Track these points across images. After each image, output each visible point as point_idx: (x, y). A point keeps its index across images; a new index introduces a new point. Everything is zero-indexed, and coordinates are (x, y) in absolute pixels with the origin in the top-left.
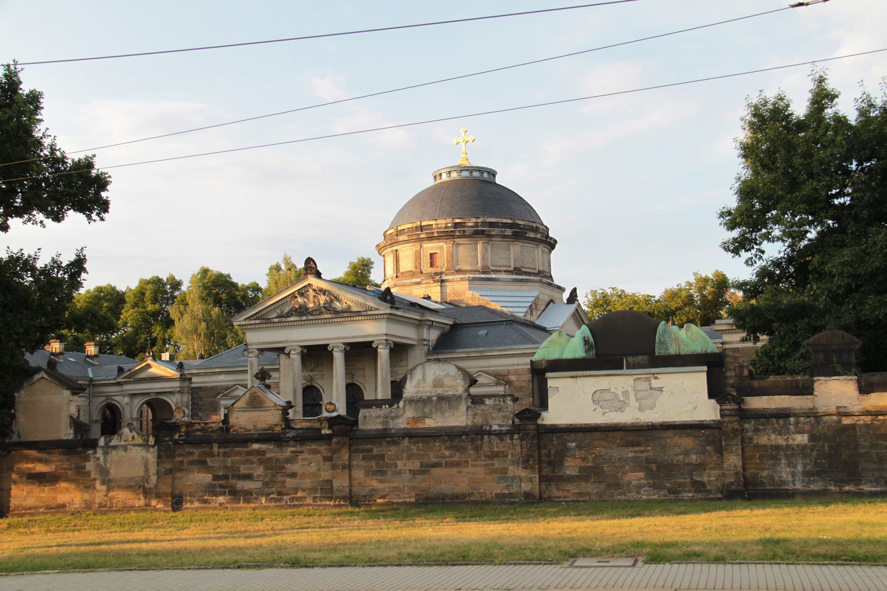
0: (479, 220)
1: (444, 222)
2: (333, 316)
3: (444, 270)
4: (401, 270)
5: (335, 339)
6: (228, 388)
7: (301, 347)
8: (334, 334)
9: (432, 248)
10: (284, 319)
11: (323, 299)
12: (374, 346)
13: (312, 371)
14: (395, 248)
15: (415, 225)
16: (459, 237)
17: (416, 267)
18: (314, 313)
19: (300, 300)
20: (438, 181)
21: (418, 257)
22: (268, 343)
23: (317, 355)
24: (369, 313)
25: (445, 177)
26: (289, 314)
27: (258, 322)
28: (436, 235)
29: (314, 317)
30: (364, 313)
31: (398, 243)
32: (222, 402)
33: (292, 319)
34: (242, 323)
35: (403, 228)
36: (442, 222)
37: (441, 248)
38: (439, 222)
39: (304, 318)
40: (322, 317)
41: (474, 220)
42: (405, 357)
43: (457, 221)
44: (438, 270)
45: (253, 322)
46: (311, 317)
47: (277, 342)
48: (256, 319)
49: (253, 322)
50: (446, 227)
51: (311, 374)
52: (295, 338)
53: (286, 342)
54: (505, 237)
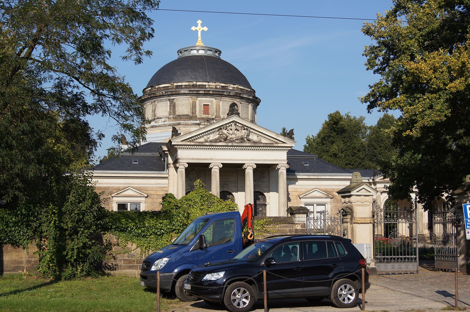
0: (235, 86)
1: (214, 84)
3: (214, 117)
4: (177, 113)
6: (119, 189)
8: (249, 158)
9: (206, 101)
10: (214, 144)
11: (243, 133)
14: (173, 98)
15: (191, 84)
16: (226, 96)
17: (193, 113)
18: (237, 141)
19: (225, 131)
21: (194, 106)
23: (233, 172)
24: (279, 145)
26: (216, 141)
28: (211, 92)
30: (276, 145)
32: (114, 199)
34: (179, 143)
35: (180, 84)
36: (213, 84)
37: (212, 102)
38: (210, 84)
39: (230, 144)
41: (232, 86)
44: (210, 116)
45: (189, 143)
47: (204, 159)
50: (216, 88)
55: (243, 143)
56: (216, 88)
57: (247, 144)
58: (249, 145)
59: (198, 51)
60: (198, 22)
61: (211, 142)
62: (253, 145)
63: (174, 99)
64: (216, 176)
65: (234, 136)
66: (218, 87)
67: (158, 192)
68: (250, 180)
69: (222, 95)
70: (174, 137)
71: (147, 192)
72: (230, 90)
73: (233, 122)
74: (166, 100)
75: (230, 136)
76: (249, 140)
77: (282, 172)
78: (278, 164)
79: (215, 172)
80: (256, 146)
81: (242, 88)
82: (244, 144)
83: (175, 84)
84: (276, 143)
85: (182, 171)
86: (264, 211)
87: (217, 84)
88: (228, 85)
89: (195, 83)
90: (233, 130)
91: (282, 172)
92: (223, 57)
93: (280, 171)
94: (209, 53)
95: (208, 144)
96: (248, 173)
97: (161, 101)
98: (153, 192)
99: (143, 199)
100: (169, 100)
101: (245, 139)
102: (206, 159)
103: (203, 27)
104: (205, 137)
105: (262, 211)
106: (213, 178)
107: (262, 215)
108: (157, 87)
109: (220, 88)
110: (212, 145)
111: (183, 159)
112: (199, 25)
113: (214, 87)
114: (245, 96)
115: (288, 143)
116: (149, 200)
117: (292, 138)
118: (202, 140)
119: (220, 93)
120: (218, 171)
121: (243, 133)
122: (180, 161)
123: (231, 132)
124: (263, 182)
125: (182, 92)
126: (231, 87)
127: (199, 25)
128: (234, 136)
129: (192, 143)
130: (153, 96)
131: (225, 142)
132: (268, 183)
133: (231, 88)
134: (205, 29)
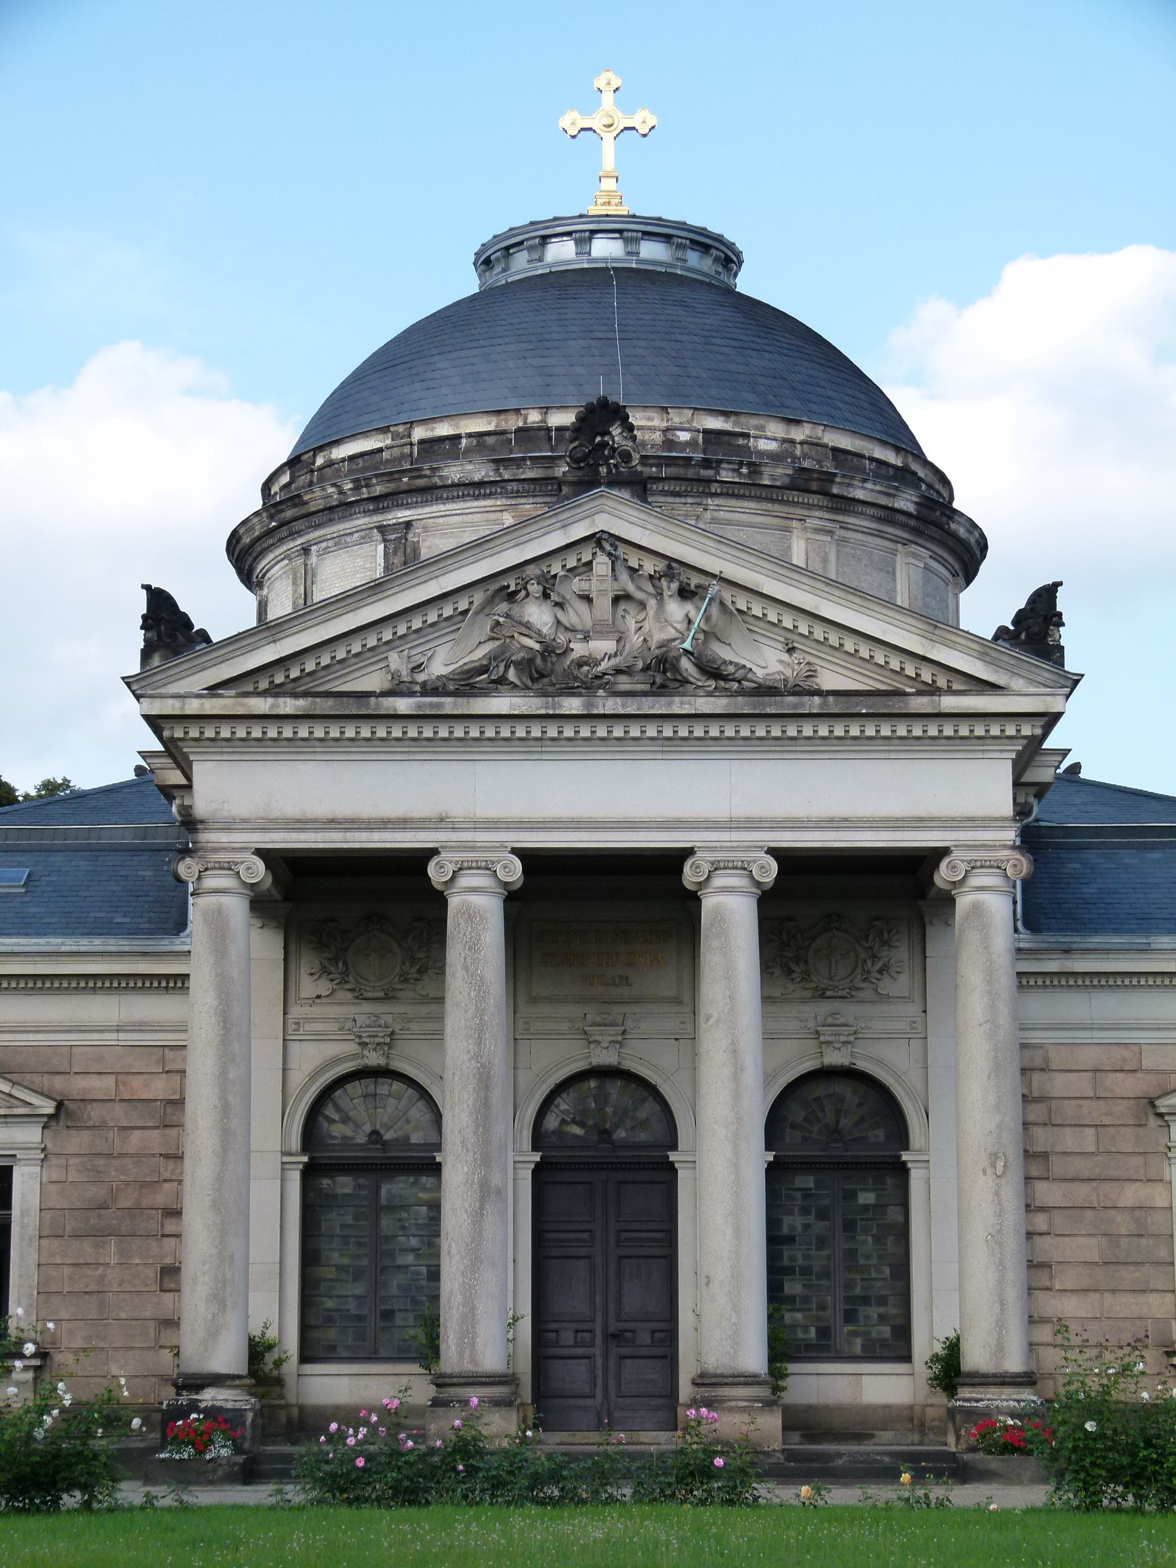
0: (799, 434)
2: (742, 705)
5: (732, 825)
7: (524, 855)
10: (449, 705)
12: (944, 874)
13: (388, 997)
14: (403, 515)
15: (513, 423)
16: (730, 491)
18: (624, 683)
19: (538, 615)
20: (498, 277)
22: (332, 823)
23: (602, 910)
24: (949, 703)
25: (521, 265)
26: (467, 683)
27: (288, 705)
29: (612, 705)
30: (920, 704)
31: (430, 492)
33: (500, 704)
34: (193, 707)
35: (443, 429)
39: (572, 705)
40: (678, 705)
41: (776, 429)
42: (901, 953)
43: (715, 423)
45: (261, 705)
46: (612, 705)
47: (385, 824)
48: (275, 691)
49: (261, 705)
51: (387, 1012)
52: (485, 810)
53: (441, 822)
54: (889, 515)
55: (680, 689)
56: (669, 444)
57: (704, 705)
58: (718, 705)
59: (583, 240)
60: (600, 82)
61: (430, 690)
62: (742, 705)
63: (408, 525)
64: (474, 946)
65: (602, 646)
66: (684, 436)
67: (136, 1082)
68: (729, 975)
69: (709, 481)
70: (156, 661)
71: (59, 1083)
72: (762, 454)
73: (596, 539)
74: (366, 539)
75: (579, 649)
76: (713, 671)
77: (976, 908)
78: (944, 852)
79: (470, 915)
80: (776, 713)
81: (844, 442)
82: (678, 705)
83: (419, 433)
84: (932, 690)
85: (219, 911)
86: (893, 1214)
87: (676, 418)
88: (749, 424)
89: (534, 417)
90: (603, 604)
91: (976, 908)
92: (747, 283)
93: (963, 902)
94: (652, 251)
95: (403, 705)
96: (720, 915)
97: (340, 542)
98: (101, 1086)
99: (31, 1134)
100: (382, 529)
101: (686, 664)
102: (403, 824)
103: (629, 112)
104: (395, 661)
105: (879, 1208)
106: (455, 954)
107: (878, 1240)
108: (320, 461)
109: (692, 444)
110: (439, 715)
111: (229, 826)
112: (608, 98)
113: (658, 437)
114: (860, 494)
115: (1018, 684)
116: (76, 1141)
117: (1053, 654)
118: (372, 681)
119: (690, 473)
120: (491, 908)
121: (671, 622)
122: (207, 837)
123: (577, 615)
124: (887, 999)
125: (454, 472)
126: (769, 436)
127: (608, 98)
128: (602, 646)
129: (288, 705)
130: (289, 514)
131: (548, 686)
132: (914, 1009)
133: (772, 446)
134: (642, 119)
